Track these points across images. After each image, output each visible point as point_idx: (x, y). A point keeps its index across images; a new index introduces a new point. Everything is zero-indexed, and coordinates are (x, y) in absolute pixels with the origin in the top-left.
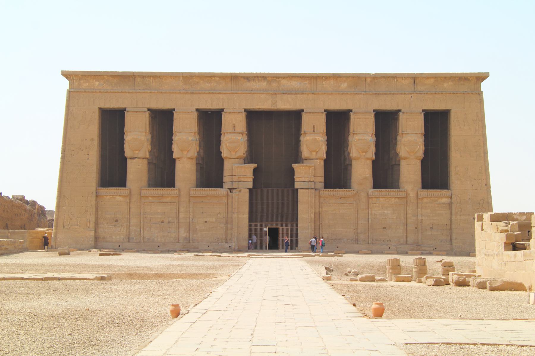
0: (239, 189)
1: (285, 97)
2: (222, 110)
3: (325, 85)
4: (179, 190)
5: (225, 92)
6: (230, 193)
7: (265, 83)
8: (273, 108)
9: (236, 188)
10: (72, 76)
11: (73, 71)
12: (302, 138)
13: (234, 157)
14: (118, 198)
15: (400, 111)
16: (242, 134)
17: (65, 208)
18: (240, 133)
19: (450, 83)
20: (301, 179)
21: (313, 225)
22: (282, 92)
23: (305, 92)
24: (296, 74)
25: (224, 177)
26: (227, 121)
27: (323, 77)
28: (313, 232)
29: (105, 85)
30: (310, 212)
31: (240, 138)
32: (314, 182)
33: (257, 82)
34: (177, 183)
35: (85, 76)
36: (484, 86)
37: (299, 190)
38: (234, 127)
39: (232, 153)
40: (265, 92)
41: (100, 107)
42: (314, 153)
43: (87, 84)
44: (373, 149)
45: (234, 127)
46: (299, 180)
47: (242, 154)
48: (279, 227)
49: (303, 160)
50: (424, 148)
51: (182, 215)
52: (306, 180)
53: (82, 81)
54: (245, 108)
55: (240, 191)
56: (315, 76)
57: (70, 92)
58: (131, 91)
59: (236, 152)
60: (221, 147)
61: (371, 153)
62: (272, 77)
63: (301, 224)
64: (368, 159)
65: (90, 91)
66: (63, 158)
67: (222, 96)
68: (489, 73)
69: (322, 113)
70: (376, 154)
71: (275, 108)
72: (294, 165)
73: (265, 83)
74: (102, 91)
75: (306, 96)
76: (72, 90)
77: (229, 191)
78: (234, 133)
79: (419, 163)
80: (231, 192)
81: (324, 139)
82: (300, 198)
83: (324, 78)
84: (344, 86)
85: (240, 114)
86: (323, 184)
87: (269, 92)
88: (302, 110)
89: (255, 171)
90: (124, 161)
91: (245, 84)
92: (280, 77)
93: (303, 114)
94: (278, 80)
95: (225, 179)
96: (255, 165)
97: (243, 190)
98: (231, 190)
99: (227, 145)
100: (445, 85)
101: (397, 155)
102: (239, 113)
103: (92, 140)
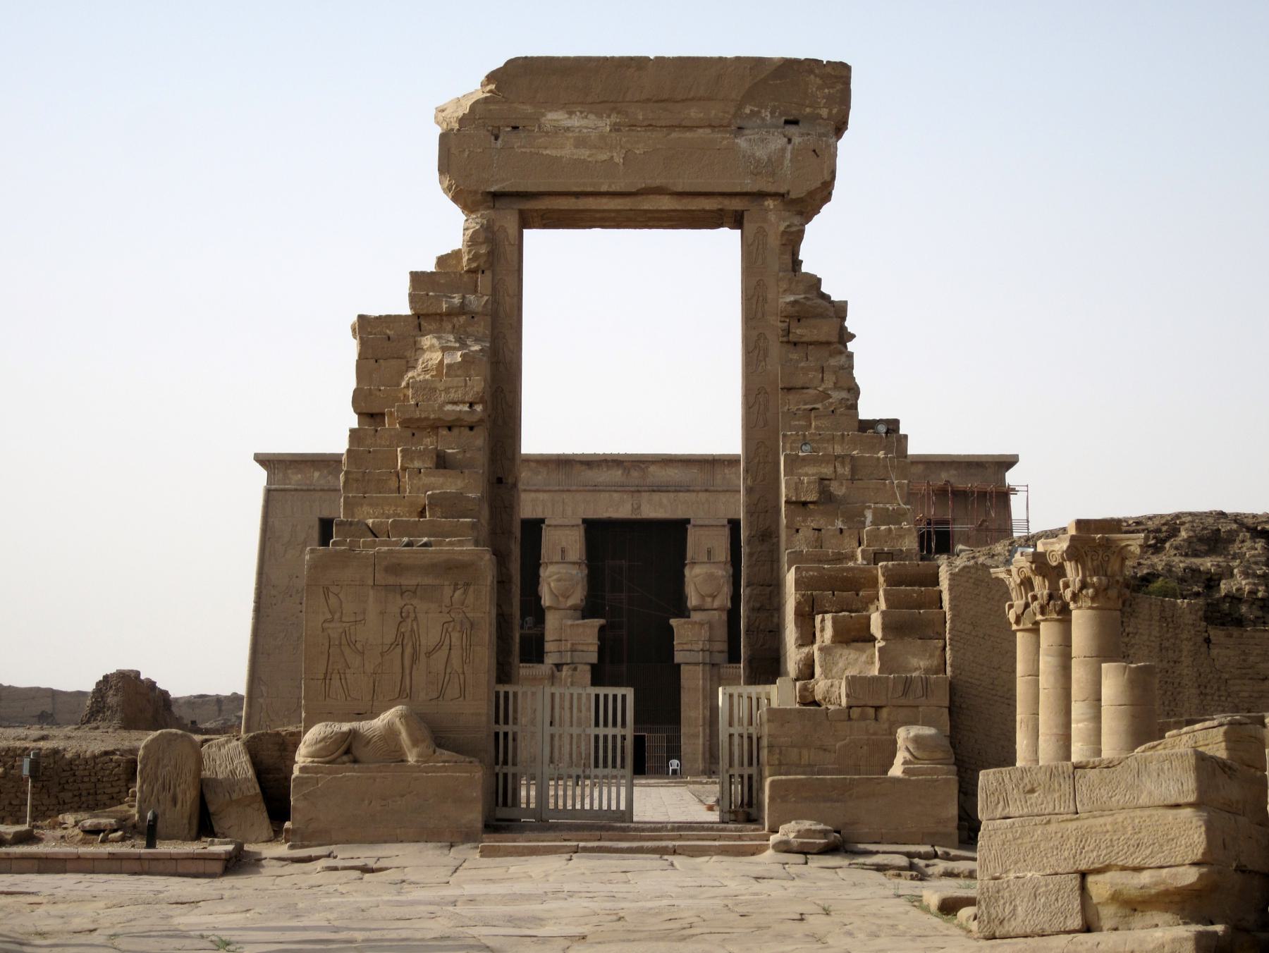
0: (573, 666)
1: (656, 496)
2: (542, 521)
3: (728, 476)
5: (548, 488)
6: (557, 674)
7: (620, 472)
8: (634, 517)
9: (567, 664)
10: (274, 465)
11: (274, 454)
12: (687, 572)
13: (562, 606)
16: (579, 564)
17: (261, 700)
18: (574, 563)
19: (953, 472)
20: (686, 647)
21: (708, 731)
22: (651, 488)
23: (691, 488)
24: (676, 455)
25: (546, 644)
26: (551, 540)
27: (724, 461)
28: (708, 743)
29: (330, 477)
30: (701, 707)
31: (574, 572)
32: (708, 653)
33: (605, 469)
35: (296, 461)
36: (1012, 477)
38: (563, 551)
39: (560, 599)
40: (620, 489)
41: (321, 516)
42: (709, 600)
43: (299, 476)
45: (563, 551)
46: (681, 648)
47: (579, 602)
48: (646, 735)
49: (689, 611)
52: (695, 647)
53: (289, 471)
54: (584, 517)
55: (575, 669)
56: (711, 458)
57: (269, 493)
59: (568, 597)
60: (540, 588)
62: (632, 461)
63: (684, 730)
65: (305, 488)
67: (541, 496)
68: (1018, 455)
69: (724, 526)
71: (639, 517)
72: (673, 622)
73: (620, 472)
74: (326, 488)
75: (694, 495)
76: (273, 487)
77: (555, 669)
78: (563, 563)
80: (558, 671)
81: (727, 572)
82: (684, 682)
83: (726, 463)
85: (575, 528)
86: (725, 655)
87: (627, 488)
88: (687, 521)
91: (583, 473)
92: (647, 461)
93: (689, 527)
94: (643, 466)
95: (549, 646)
96: (602, 621)
97: (580, 667)
98: (559, 666)
99: (552, 585)
102: (573, 526)
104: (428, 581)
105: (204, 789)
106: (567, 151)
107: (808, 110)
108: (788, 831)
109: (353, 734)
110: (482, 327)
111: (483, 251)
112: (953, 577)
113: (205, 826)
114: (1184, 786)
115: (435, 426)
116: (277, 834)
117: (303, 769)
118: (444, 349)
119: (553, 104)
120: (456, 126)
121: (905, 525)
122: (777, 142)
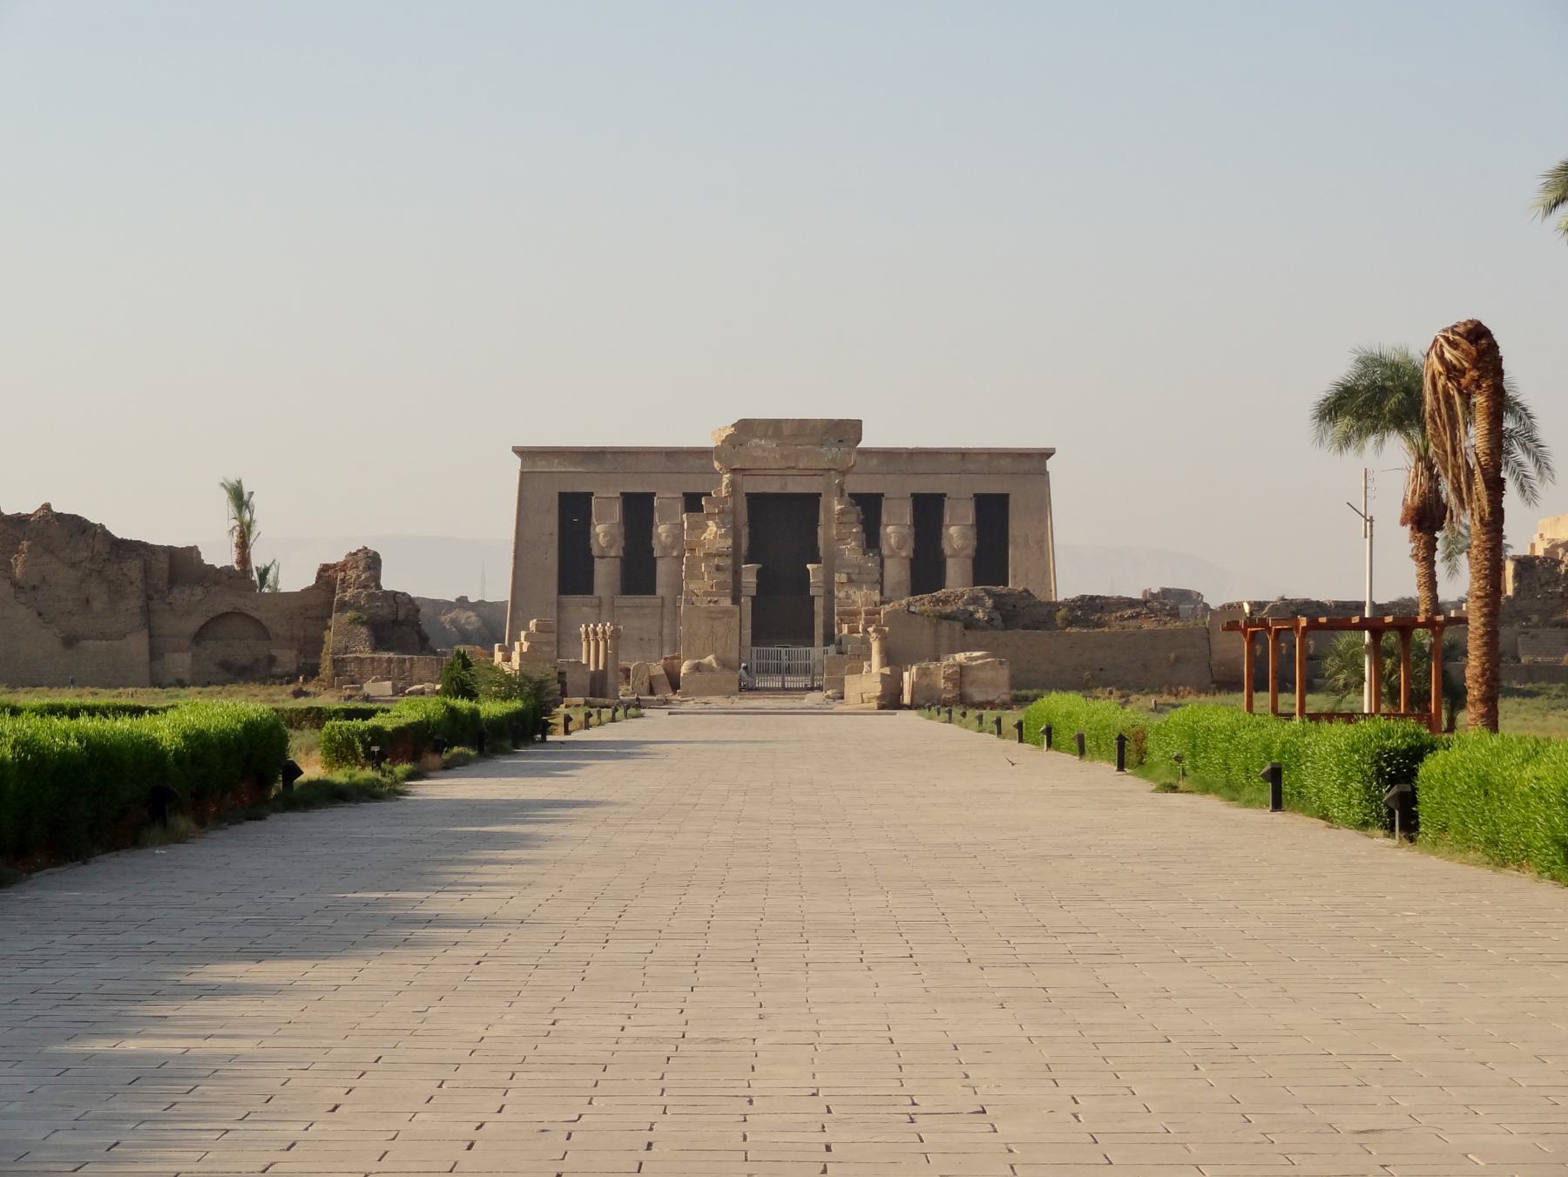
4: (662, 598)
14: (585, 609)
15: (945, 495)
19: (1009, 460)
34: (660, 591)
36: (1051, 464)
37: (816, 600)
44: (910, 544)
50: (975, 543)
51: (666, 631)
57: (522, 473)
58: (600, 471)
61: (906, 552)
64: (903, 557)
66: (516, 558)
70: (914, 551)
72: (809, 566)
76: (526, 470)
79: (969, 562)
84: (874, 462)
89: (759, 574)
90: (591, 559)
96: (760, 566)
100: (1002, 462)
101: (943, 550)
103: (551, 534)
104: (721, 616)
105: (651, 679)
106: (759, 453)
107: (846, 437)
108: (829, 693)
109: (699, 663)
110: (730, 518)
111: (730, 489)
112: (884, 614)
113: (652, 692)
114: (879, 679)
115: (714, 556)
116: (675, 693)
117: (684, 674)
118: (718, 528)
119: (756, 437)
120: (720, 444)
121: (877, 591)
122: (835, 450)
